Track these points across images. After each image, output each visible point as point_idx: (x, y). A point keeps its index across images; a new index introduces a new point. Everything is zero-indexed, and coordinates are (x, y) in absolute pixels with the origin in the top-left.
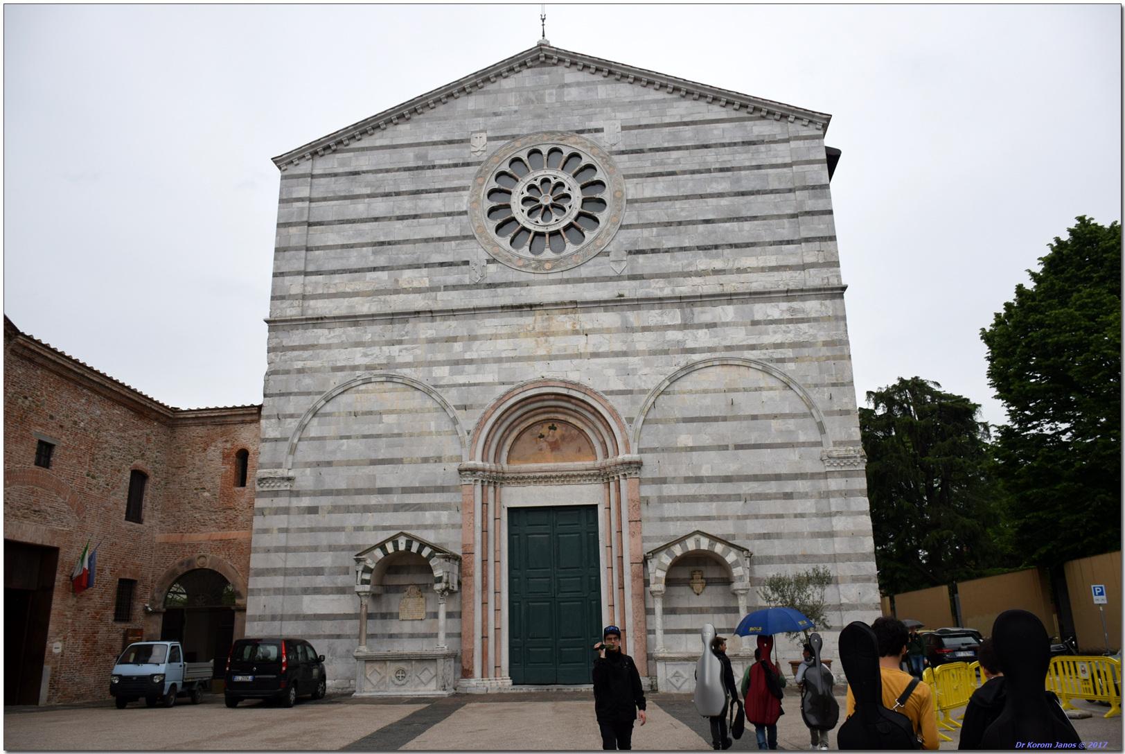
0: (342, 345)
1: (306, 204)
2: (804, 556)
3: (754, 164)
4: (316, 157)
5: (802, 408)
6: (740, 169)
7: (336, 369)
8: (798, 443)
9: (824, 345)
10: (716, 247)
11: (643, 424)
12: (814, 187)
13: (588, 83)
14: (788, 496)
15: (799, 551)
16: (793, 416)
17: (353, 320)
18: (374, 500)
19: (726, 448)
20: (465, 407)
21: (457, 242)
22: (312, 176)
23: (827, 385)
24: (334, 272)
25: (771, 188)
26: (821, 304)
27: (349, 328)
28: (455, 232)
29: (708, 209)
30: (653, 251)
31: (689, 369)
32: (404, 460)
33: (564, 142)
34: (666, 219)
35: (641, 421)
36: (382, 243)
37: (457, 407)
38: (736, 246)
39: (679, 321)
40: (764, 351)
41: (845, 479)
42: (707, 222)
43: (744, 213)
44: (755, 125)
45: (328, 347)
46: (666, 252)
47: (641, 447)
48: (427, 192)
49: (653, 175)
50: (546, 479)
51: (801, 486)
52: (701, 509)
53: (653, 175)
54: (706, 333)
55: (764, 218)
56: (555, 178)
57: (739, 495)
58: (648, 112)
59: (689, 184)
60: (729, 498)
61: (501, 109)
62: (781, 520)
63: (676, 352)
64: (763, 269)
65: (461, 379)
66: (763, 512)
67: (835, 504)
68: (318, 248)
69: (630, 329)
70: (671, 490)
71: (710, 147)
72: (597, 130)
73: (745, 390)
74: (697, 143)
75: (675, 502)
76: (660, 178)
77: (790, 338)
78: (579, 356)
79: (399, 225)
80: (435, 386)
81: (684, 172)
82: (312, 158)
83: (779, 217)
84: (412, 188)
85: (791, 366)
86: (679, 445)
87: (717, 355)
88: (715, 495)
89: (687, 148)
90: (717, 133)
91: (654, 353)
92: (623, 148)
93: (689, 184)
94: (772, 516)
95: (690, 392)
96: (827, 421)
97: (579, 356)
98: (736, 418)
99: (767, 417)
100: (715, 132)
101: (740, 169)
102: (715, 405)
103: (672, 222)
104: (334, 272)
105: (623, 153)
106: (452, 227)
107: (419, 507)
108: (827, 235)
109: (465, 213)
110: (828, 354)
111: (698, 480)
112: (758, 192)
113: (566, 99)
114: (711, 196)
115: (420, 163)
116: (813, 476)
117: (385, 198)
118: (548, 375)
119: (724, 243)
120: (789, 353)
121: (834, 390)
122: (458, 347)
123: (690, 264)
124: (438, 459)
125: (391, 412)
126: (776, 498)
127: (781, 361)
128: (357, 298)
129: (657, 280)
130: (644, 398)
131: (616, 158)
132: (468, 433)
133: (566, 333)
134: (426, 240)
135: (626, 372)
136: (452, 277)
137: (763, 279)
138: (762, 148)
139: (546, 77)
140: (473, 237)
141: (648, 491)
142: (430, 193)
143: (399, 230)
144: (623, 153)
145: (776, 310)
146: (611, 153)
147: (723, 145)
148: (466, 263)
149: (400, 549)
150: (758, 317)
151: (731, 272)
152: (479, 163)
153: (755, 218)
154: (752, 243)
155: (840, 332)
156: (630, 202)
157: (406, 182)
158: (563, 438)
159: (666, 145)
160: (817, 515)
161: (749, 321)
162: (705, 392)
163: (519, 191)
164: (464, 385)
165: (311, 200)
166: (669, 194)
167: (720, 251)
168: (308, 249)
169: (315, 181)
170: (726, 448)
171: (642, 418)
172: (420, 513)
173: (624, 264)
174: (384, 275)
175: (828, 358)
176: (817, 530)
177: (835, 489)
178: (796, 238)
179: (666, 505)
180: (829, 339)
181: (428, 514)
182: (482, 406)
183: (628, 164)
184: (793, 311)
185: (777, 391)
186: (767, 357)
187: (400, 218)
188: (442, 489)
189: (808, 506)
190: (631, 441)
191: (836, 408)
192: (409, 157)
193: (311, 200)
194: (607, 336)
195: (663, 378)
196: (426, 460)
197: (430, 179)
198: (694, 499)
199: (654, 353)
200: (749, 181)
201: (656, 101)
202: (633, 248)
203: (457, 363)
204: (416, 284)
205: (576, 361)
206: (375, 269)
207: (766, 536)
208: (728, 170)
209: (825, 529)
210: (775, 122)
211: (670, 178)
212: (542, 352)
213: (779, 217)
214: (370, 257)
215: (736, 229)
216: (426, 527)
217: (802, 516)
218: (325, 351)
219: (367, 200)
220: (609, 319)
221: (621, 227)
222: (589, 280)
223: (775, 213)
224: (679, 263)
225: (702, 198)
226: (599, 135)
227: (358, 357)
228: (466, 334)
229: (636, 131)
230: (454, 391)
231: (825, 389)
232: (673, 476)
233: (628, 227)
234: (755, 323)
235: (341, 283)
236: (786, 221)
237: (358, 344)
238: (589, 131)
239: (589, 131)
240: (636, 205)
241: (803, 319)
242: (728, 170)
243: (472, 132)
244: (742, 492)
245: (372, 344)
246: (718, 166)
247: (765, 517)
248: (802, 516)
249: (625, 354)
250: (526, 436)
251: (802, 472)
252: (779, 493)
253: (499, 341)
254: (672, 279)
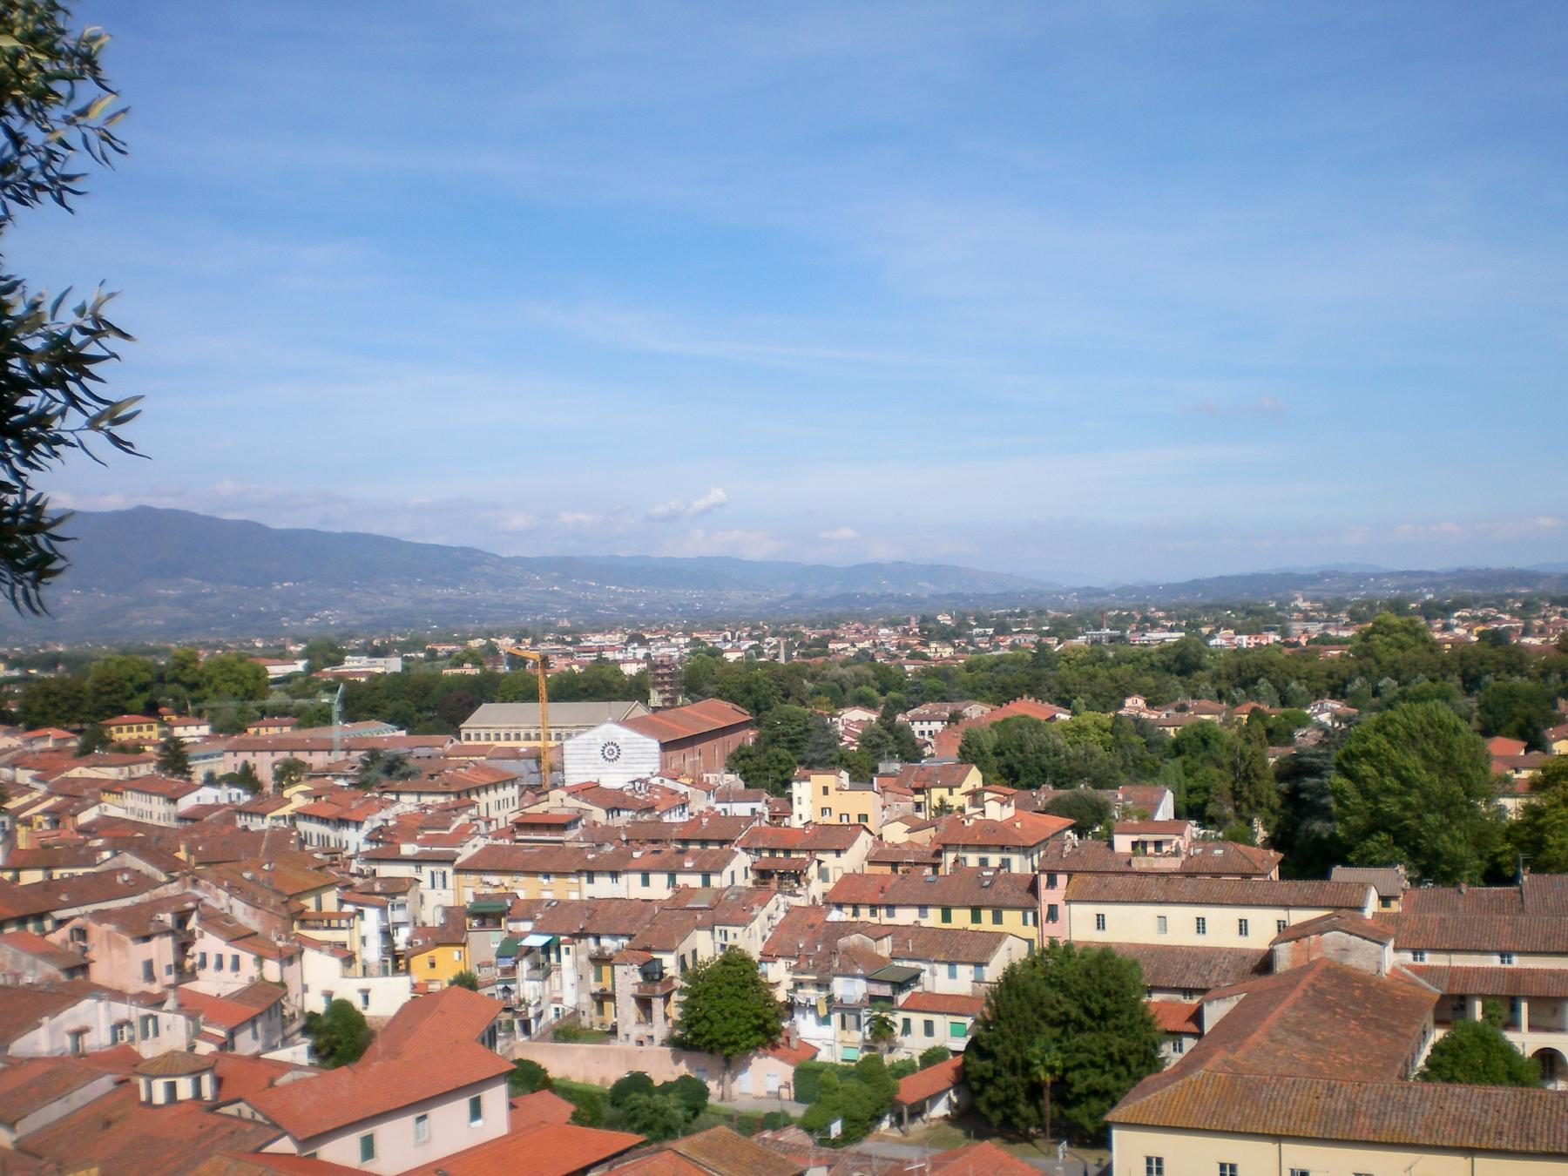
90: (641, 741)
157: (586, 747)
192: (586, 742)
197: (591, 746)
200: (644, 750)
214: (581, 762)
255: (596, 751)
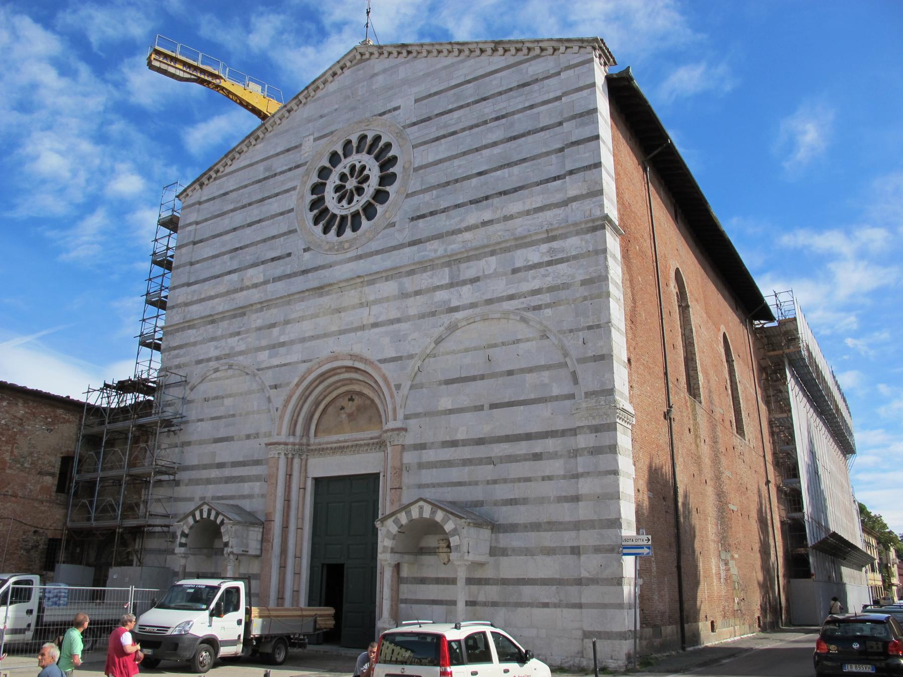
0: (204, 341)
1: (194, 227)
2: (549, 523)
3: (527, 104)
4: (204, 187)
5: (558, 358)
6: (513, 113)
7: (199, 362)
8: (551, 397)
9: (581, 285)
10: (487, 198)
11: (410, 390)
12: (581, 115)
13: (392, 67)
14: (537, 457)
15: (544, 518)
16: (548, 367)
17: (212, 320)
18: (214, 473)
19: (480, 408)
20: (276, 387)
21: (285, 237)
22: (200, 203)
23: (583, 329)
24: (205, 280)
25: (541, 125)
26: (582, 240)
27: (209, 326)
28: (285, 229)
29: (481, 161)
30: (432, 214)
31: (453, 328)
32: (235, 438)
33: (370, 127)
34: (444, 180)
35: (408, 387)
36: (236, 249)
37: (271, 387)
38: (505, 193)
39: (446, 281)
40: (523, 300)
41: (594, 435)
42: (480, 174)
43: (516, 158)
44: (530, 65)
45: (195, 344)
46: (443, 212)
47: (407, 413)
48: (269, 197)
49: (438, 139)
50: (341, 449)
51: (550, 445)
52: (455, 474)
53: (438, 139)
54: (469, 289)
55: (533, 158)
56: (360, 162)
57: (491, 458)
58: (437, 80)
59: (467, 140)
60: (480, 462)
61: (326, 112)
62: (528, 484)
63: (442, 313)
64: (528, 213)
65: (276, 361)
66: (513, 476)
67: (582, 463)
68: (198, 262)
69: (404, 295)
70: (430, 455)
71: (488, 99)
72: (396, 109)
73: (503, 344)
74: (477, 98)
75: (433, 468)
76: (443, 141)
77: (549, 281)
78: (362, 328)
79: (248, 231)
80: (258, 370)
81: (464, 130)
82: (202, 189)
83: (547, 154)
84: (259, 197)
85: (548, 312)
86: (440, 408)
87: (478, 310)
88: (468, 459)
89: (468, 105)
91: (422, 316)
92: (414, 120)
93: (467, 140)
94: (519, 480)
95: (453, 352)
96: (580, 369)
97: (362, 328)
98: (493, 375)
99: (523, 371)
100: (494, 83)
101: (513, 113)
102: (471, 363)
103: (449, 182)
104: (205, 280)
105: (414, 124)
106: (282, 225)
107: (242, 479)
108: (592, 162)
109: (292, 210)
110: (586, 294)
111: (454, 444)
112: (529, 133)
113: (374, 88)
114: (486, 147)
115: (267, 174)
116: (563, 433)
117: (242, 210)
118: (338, 349)
119: (494, 192)
120: (546, 298)
121: (587, 334)
122: (276, 331)
123: (461, 221)
124: (257, 436)
125: (230, 396)
126: (526, 460)
127: (538, 308)
128: (218, 299)
129: (432, 242)
130: (412, 362)
131: (409, 130)
132: (277, 410)
133: (354, 307)
134: (264, 241)
135: (398, 338)
136: (279, 269)
137: (529, 222)
138: (535, 87)
139: (361, 72)
140: (295, 231)
141: (409, 458)
142: (271, 198)
143: (249, 235)
144: (414, 124)
145: (534, 255)
146: (404, 127)
147: (500, 93)
148: (289, 255)
149: (204, 517)
150: (519, 264)
151: (498, 221)
152: (305, 164)
153: (524, 160)
154: (519, 187)
155: (599, 267)
156: (416, 170)
157: (256, 193)
158: (359, 409)
159: (450, 107)
160: (564, 477)
161: (509, 269)
162: (467, 350)
163: (333, 180)
164: (277, 366)
165: (197, 223)
166: (449, 154)
167: (490, 201)
168: (192, 264)
169: (202, 206)
170: (480, 408)
171: (409, 383)
172: (241, 484)
173: (406, 232)
174: (235, 276)
175: (585, 299)
176: (564, 494)
177: (584, 446)
178: (563, 172)
179: (424, 471)
180: (588, 277)
181: (246, 484)
182: (288, 384)
183: (417, 135)
184: (551, 251)
185: (534, 342)
186: (525, 306)
187: (250, 225)
188: (257, 463)
189: (555, 467)
190: (398, 408)
191: (590, 354)
192: (260, 171)
193: (197, 223)
194: (386, 305)
195: (429, 340)
196: (248, 437)
198: (448, 464)
199: (422, 316)
200: (521, 123)
201: (445, 68)
202: (415, 215)
203: (273, 347)
204: (255, 281)
205: (359, 333)
206: (230, 272)
207: (513, 502)
208: (503, 117)
209: (572, 493)
210: (549, 57)
211: (452, 137)
212: (334, 328)
213: (547, 154)
215: (507, 175)
216: (243, 497)
217: (550, 478)
218: (192, 348)
219: (230, 215)
220: (389, 288)
221: (408, 196)
222: (377, 252)
223: (544, 151)
224: (452, 221)
225: (477, 151)
226: (397, 112)
227: (211, 350)
228: (282, 320)
229: (425, 101)
230: (270, 373)
231: (580, 333)
232: (432, 441)
233: (414, 194)
234: (515, 271)
235: (208, 289)
236: (553, 157)
237: (213, 339)
238: (390, 111)
239: (390, 111)
240: (421, 171)
241: (562, 259)
242: (503, 117)
243: (304, 137)
244: (493, 455)
245: (222, 337)
246: (494, 116)
247: (514, 481)
248: (550, 478)
249: (398, 320)
250: (330, 409)
251: (554, 429)
252: (528, 454)
253: (305, 322)
254: (445, 238)
255: (291, 201)
